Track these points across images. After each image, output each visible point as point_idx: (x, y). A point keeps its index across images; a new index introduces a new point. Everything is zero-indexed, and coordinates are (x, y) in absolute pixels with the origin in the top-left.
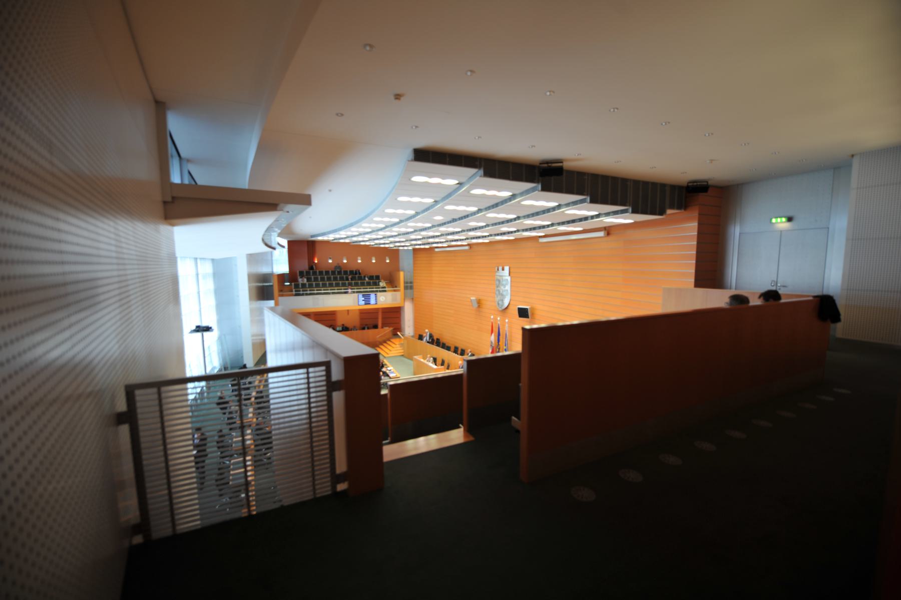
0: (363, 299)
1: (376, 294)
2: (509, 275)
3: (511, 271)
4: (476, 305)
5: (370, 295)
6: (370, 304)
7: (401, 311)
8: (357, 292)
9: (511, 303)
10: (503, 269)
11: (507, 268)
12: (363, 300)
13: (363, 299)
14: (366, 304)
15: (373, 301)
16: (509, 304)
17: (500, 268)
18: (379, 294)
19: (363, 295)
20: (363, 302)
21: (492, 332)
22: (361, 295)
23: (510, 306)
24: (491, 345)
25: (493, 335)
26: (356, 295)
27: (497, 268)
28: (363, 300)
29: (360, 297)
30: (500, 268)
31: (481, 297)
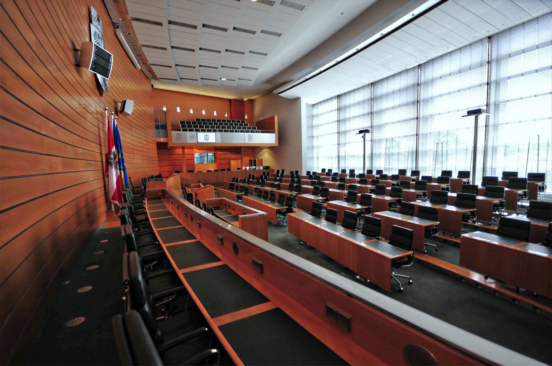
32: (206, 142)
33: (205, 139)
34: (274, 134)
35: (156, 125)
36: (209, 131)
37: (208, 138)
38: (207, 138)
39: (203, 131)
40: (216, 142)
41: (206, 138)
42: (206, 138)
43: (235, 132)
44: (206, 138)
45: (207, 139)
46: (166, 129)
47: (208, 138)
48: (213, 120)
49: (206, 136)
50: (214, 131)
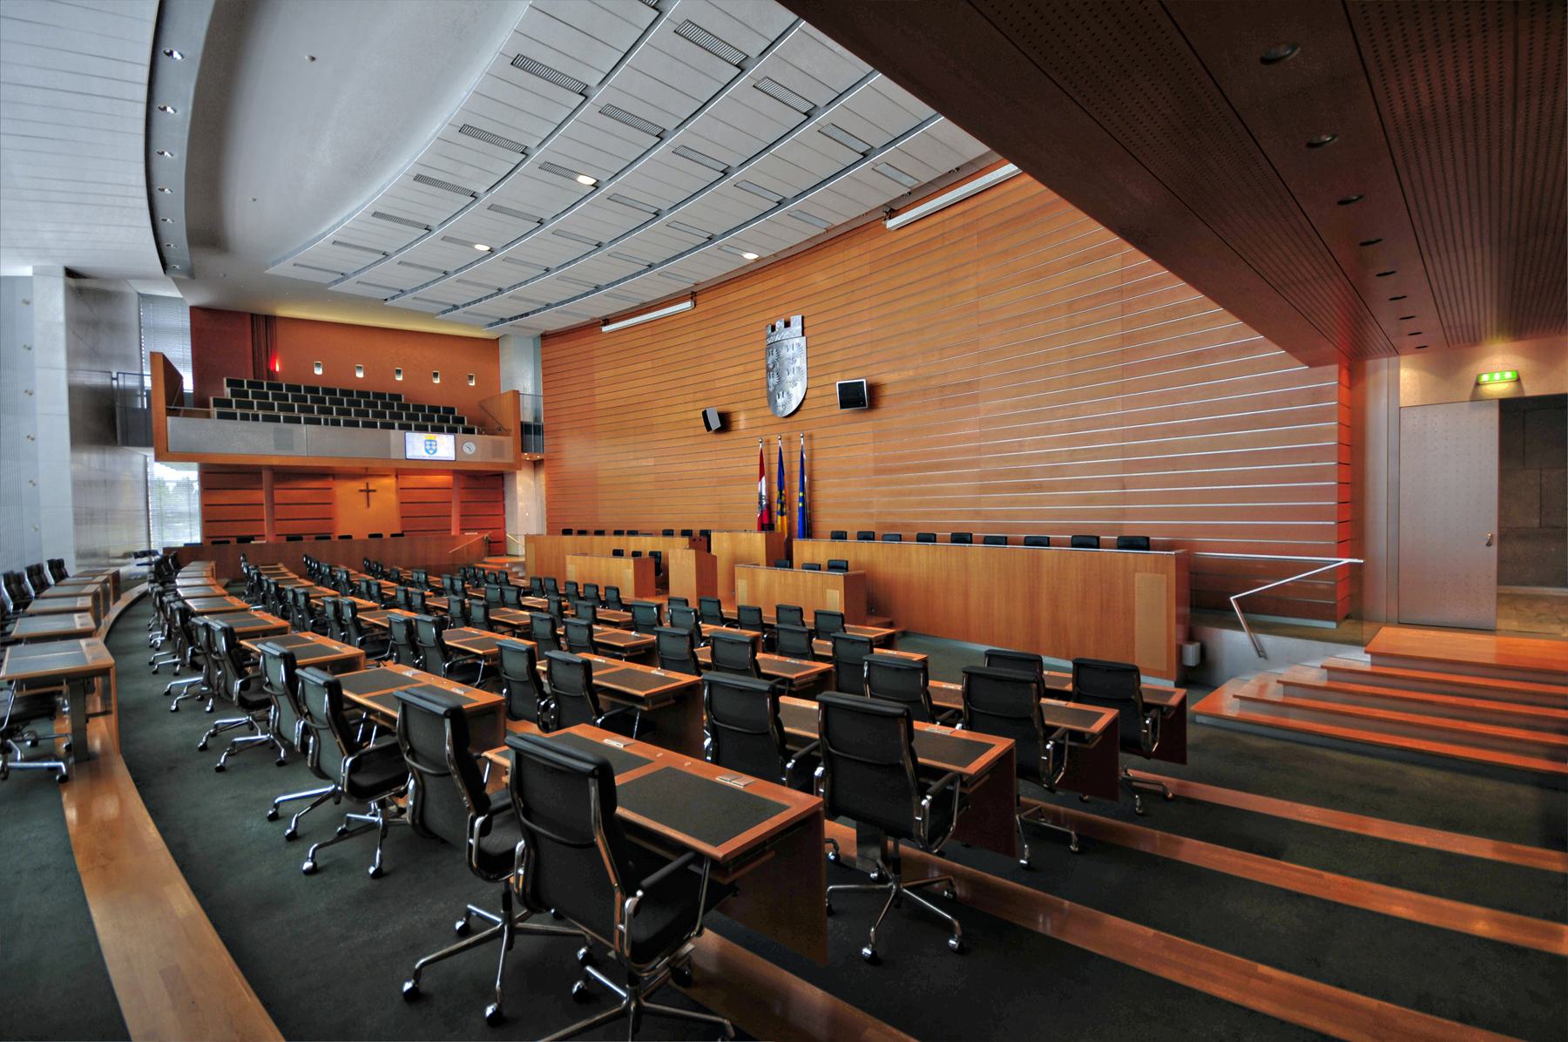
2: (803, 335)
3: (805, 325)
4: (715, 423)
7: (507, 502)
9: (811, 393)
10: (787, 324)
11: (796, 321)
16: (804, 399)
17: (780, 324)
21: (762, 474)
23: (805, 402)
24: (760, 503)
25: (764, 478)
27: (770, 328)
30: (780, 324)
31: (724, 409)
32: (427, 456)
33: (427, 451)
36: (438, 430)
37: (434, 448)
38: (431, 449)
39: (422, 429)
40: (458, 459)
41: (431, 446)
42: (431, 446)
43: (332, 424)
44: (428, 447)
45: (431, 452)
47: (434, 448)
48: (345, 393)
49: (428, 443)
50: (452, 431)
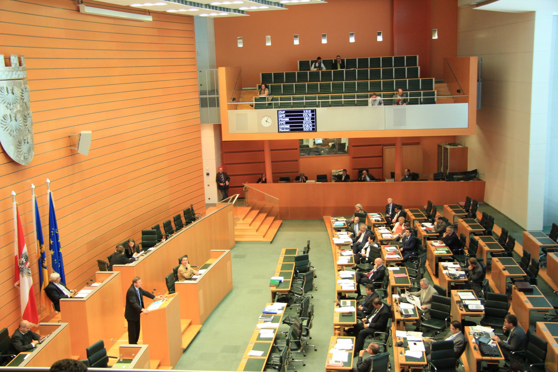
0: (287, 119)
1: (312, 111)
5: (302, 112)
6: (302, 130)
8: (276, 106)
12: (287, 123)
13: (287, 119)
14: (292, 130)
15: (307, 124)
18: (320, 111)
19: (286, 112)
20: (288, 126)
22: (282, 114)
26: (274, 111)
28: (287, 123)
29: (280, 116)
34: (467, 104)
35: (202, 100)
46: (218, 106)
